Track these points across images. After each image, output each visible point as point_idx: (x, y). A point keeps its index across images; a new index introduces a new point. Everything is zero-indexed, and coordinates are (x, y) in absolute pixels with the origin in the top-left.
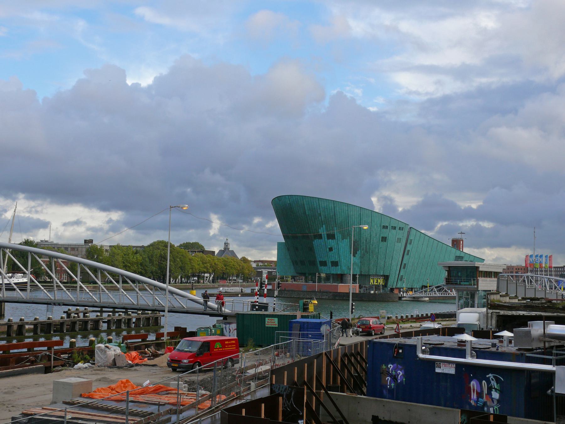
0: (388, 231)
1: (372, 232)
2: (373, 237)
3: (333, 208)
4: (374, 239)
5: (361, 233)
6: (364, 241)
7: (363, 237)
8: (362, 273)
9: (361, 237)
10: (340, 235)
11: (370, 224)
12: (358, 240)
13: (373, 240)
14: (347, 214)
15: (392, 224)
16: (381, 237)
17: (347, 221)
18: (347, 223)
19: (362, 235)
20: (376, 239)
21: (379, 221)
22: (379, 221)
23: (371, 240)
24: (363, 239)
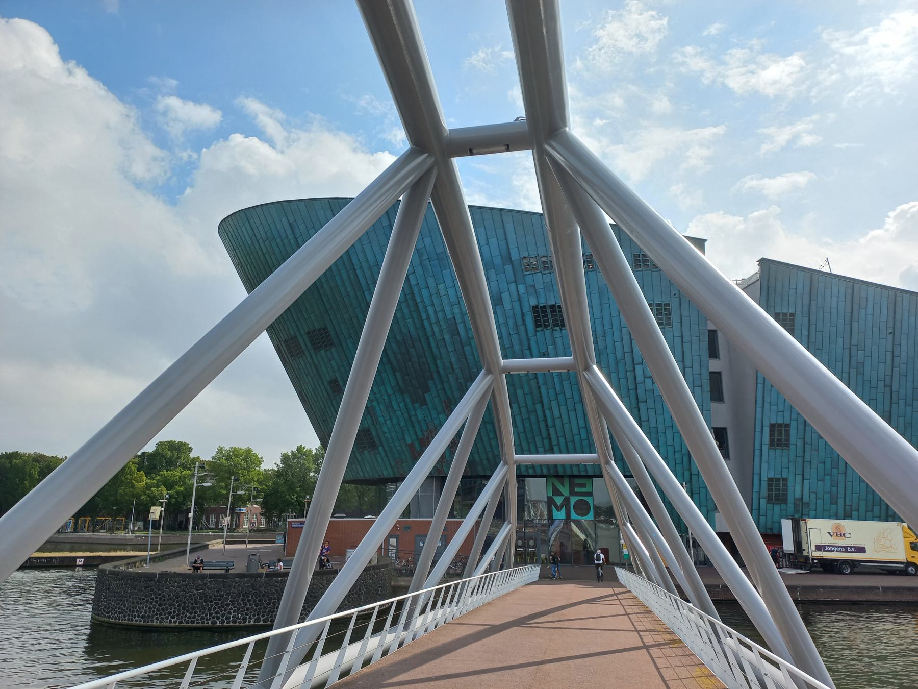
6: (447, 337)
7: (433, 319)
8: (480, 468)
9: (426, 323)
12: (413, 333)
16: (526, 309)
19: (427, 312)
22: (493, 241)
24: (436, 329)
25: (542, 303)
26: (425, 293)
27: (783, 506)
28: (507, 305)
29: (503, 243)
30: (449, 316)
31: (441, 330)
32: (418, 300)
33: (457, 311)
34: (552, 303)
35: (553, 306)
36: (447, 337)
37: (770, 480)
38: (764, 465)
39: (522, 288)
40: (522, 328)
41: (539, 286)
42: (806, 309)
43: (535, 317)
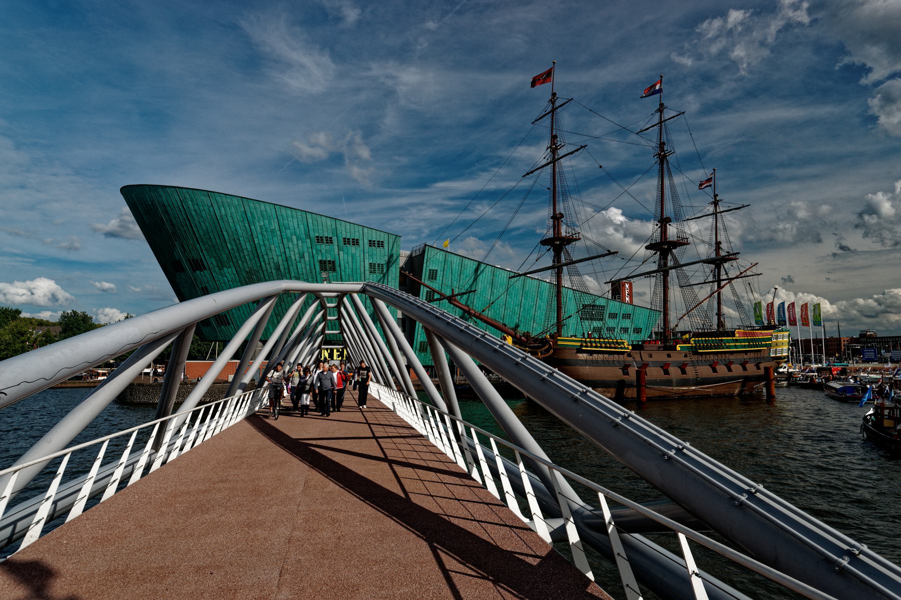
0: (336, 248)
1: (287, 250)
2: (294, 261)
3: (180, 204)
4: (299, 264)
5: (260, 254)
6: (274, 271)
7: (267, 262)
9: (263, 263)
10: (213, 260)
11: (278, 233)
13: (295, 267)
14: (213, 214)
15: (344, 232)
17: (219, 229)
18: (220, 233)
19: (263, 258)
20: (303, 266)
21: (301, 226)
22: (301, 226)
23: (291, 268)
24: (268, 267)
25: (324, 259)
26: (263, 248)
27: (426, 353)
28: (307, 259)
29: (306, 227)
30: (276, 261)
31: (271, 268)
32: (259, 251)
33: (280, 258)
34: (329, 259)
35: (329, 261)
36: (274, 271)
37: (421, 342)
38: (419, 336)
39: (314, 251)
40: (314, 270)
41: (323, 251)
42: (442, 269)
43: (320, 266)
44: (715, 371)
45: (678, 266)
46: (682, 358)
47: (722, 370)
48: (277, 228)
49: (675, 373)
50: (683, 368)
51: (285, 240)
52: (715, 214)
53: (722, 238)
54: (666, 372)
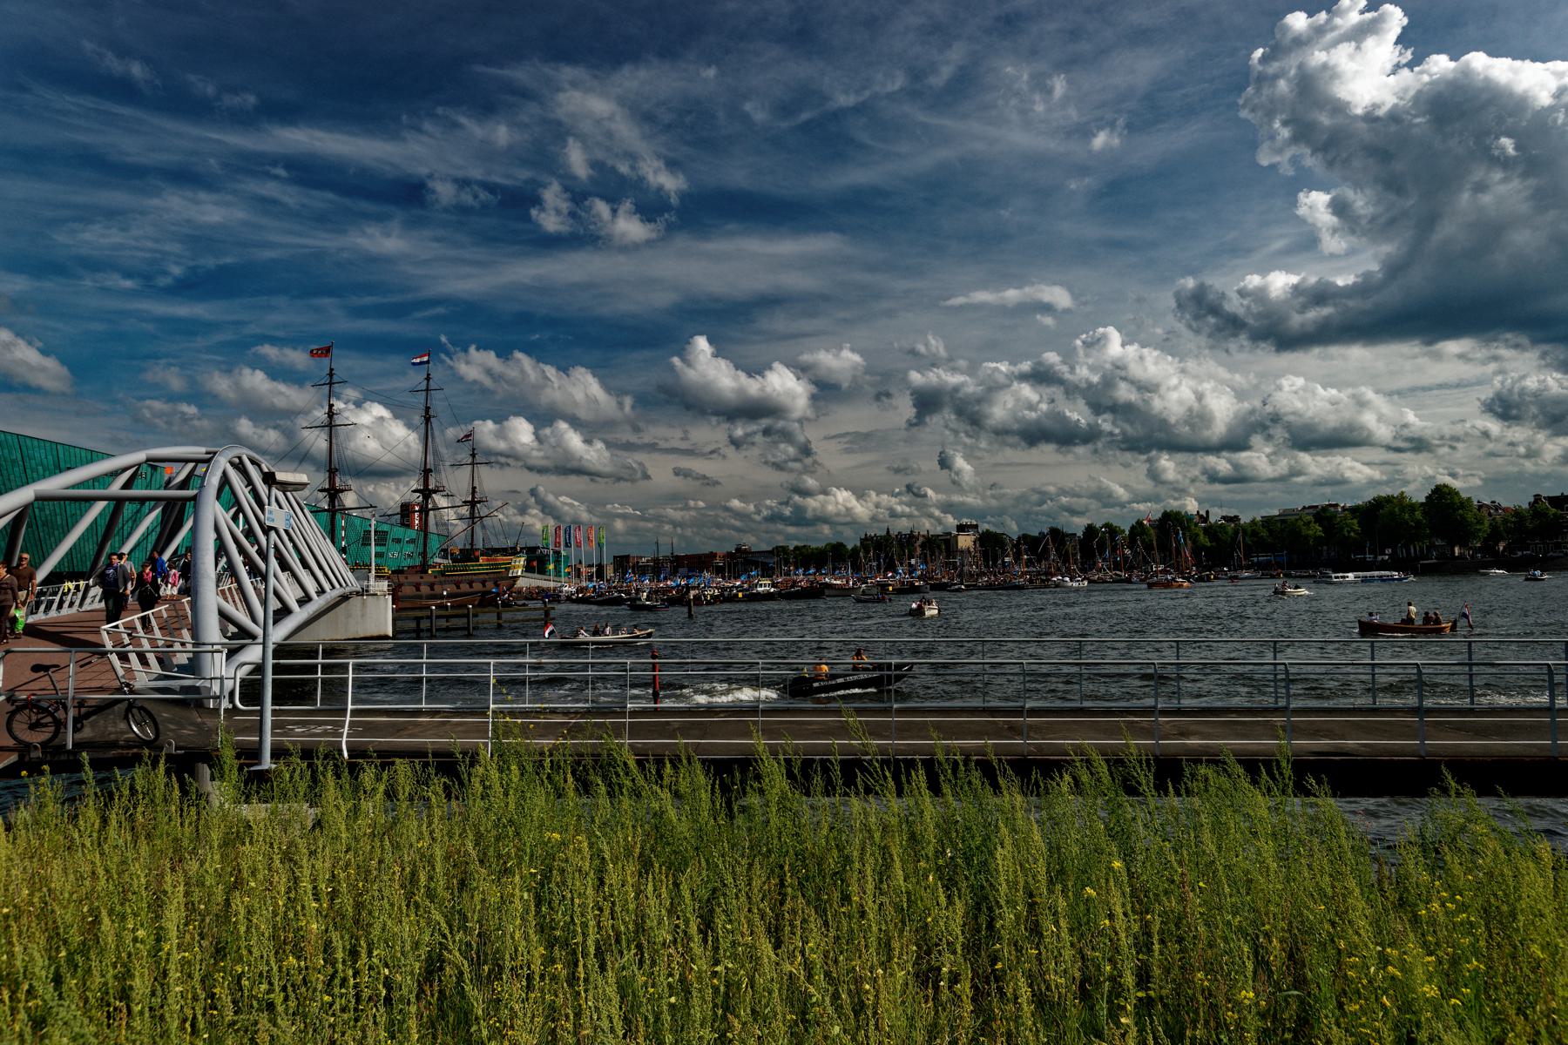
21: (50, 457)
22: (50, 457)
44: (458, 587)
45: (436, 508)
46: (432, 579)
47: (465, 587)
48: (19, 458)
49: (425, 590)
50: (432, 586)
51: (28, 471)
52: (473, 464)
53: (476, 484)
54: (418, 589)
